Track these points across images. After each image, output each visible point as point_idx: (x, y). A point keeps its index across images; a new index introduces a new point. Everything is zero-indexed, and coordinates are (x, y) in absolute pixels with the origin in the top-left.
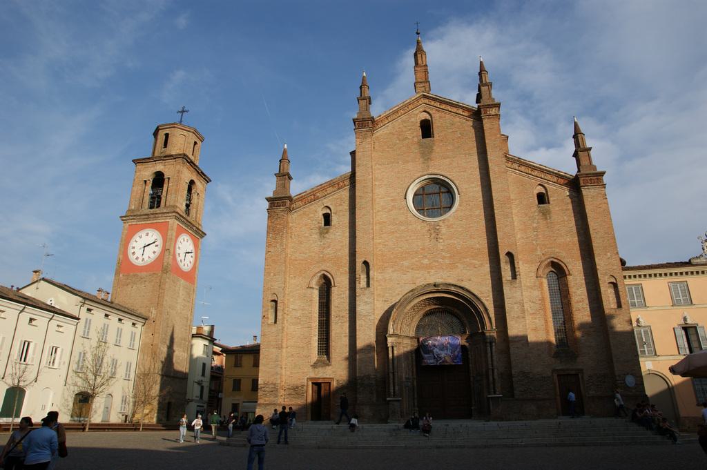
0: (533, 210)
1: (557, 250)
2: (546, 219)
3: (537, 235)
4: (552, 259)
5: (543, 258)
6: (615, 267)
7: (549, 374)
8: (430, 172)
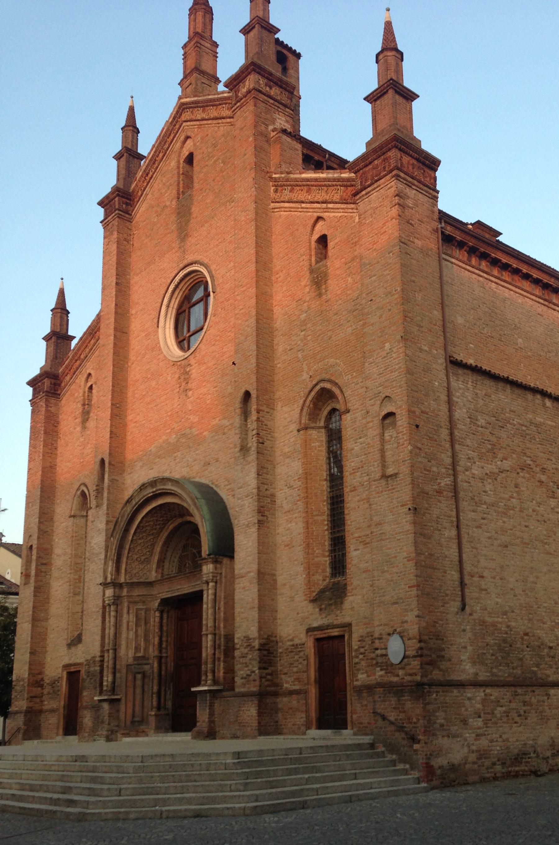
0: (303, 283)
1: (332, 361)
2: (320, 295)
3: (305, 337)
4: (322, 385)
5: (310, 386)
6: (396, 374)
7: (302, 637)
8: (186, 262)
